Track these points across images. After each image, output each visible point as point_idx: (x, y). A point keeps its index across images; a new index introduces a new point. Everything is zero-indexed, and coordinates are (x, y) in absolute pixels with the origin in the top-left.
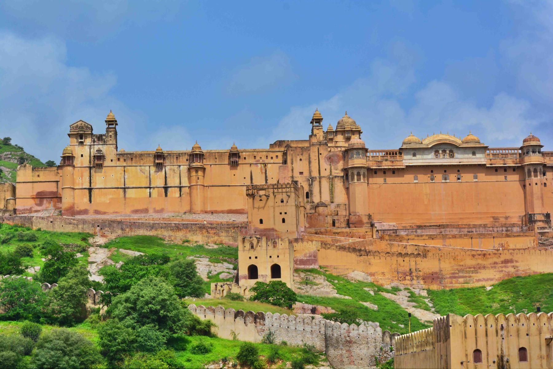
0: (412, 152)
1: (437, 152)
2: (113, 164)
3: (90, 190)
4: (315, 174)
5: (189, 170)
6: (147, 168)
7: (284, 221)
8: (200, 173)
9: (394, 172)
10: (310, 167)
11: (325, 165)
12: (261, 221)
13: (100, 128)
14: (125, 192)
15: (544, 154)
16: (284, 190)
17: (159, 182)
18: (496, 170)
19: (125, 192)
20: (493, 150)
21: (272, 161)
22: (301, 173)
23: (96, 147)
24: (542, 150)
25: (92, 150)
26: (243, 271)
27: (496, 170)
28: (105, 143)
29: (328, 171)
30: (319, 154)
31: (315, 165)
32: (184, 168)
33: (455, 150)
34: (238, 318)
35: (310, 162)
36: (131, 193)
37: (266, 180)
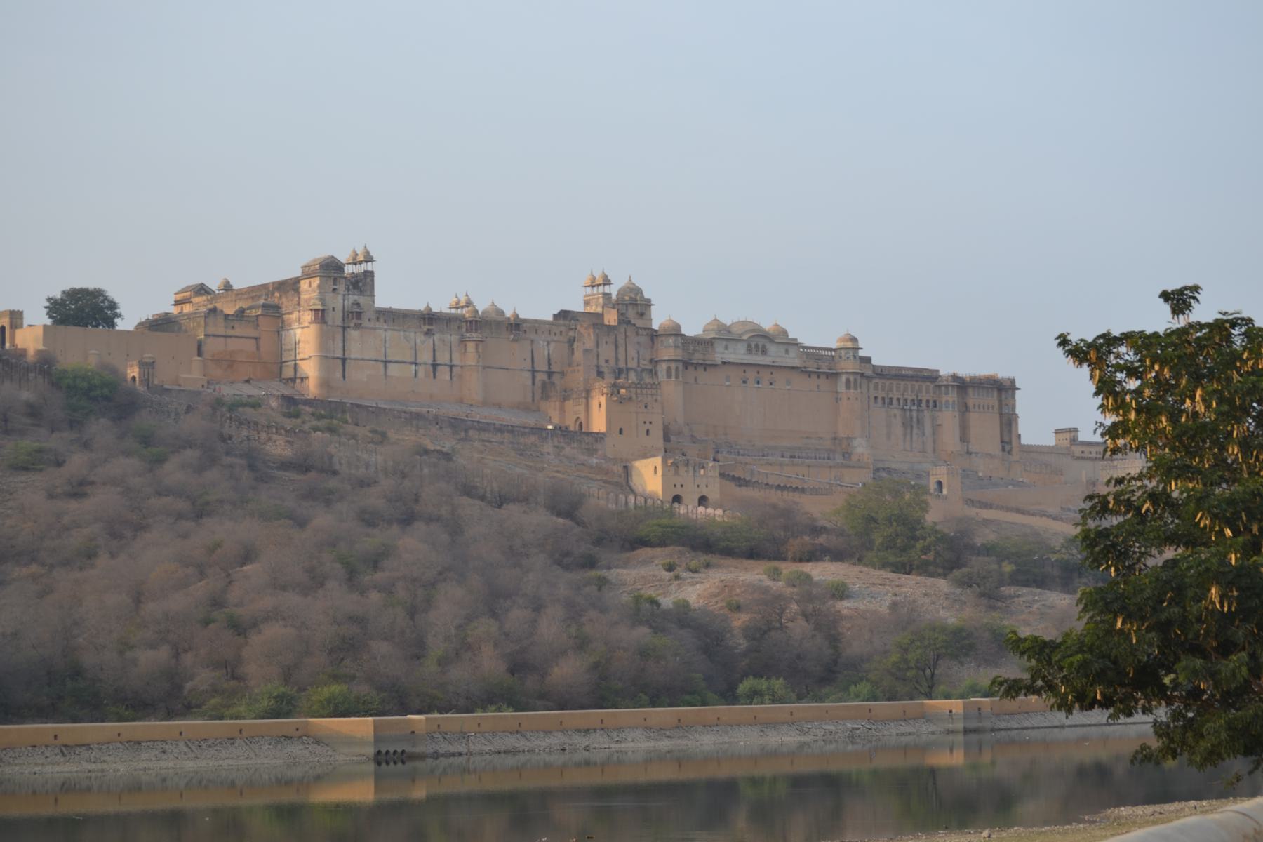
3: (344, 360)
5: (463, 341)
9: (706, 367)
11: (632, 352)
13: (349, 269)
14: (386, 367)
18: (810, 374)
19: (386, 367)
22: (607, 361)
23: (352, 298)
24: (861, 353)
27: (810, 374)
28: (361, 293)
31: (621, 350)
32: (455, 338)
33: (768, 346)
35: (617, 347)
36: (393, 370)
37: (549, 364)
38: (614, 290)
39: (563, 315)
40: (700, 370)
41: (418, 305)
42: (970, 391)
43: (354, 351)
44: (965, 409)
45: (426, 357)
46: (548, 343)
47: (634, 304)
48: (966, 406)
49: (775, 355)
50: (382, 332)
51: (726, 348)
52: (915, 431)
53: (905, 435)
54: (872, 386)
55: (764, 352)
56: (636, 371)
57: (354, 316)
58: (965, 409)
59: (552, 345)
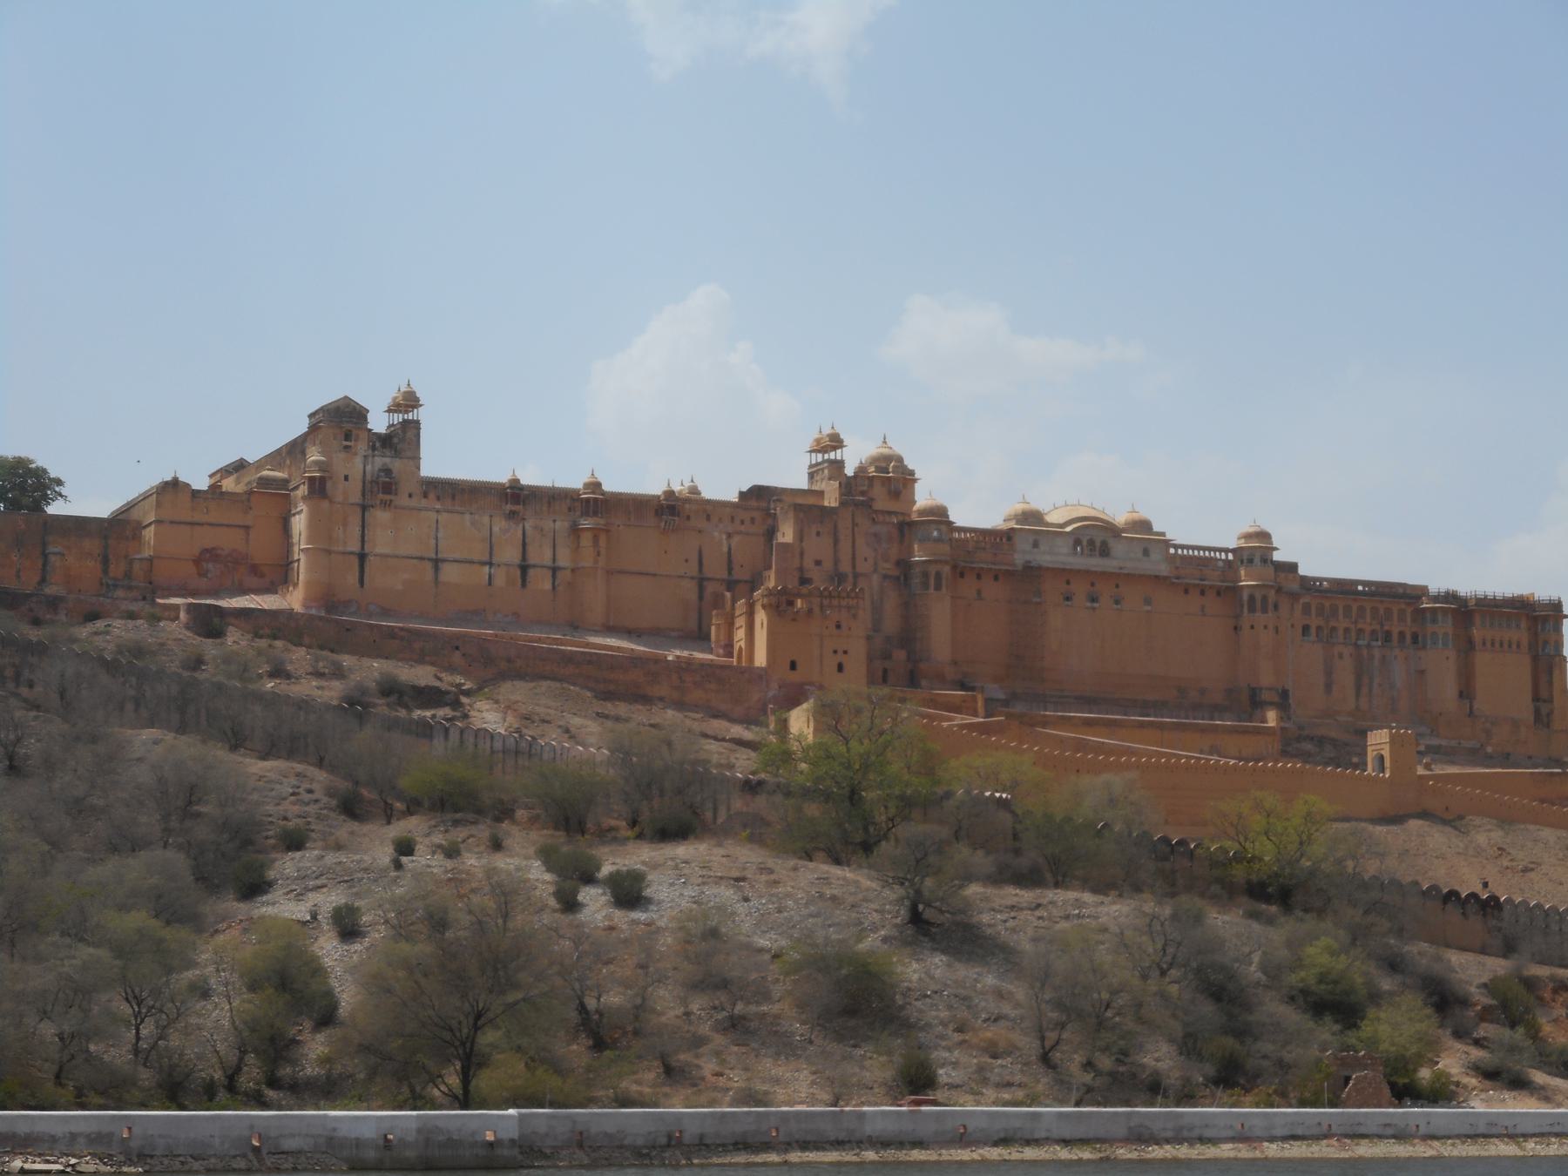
2: (413, 503)
4: (845, 567)
5: (575, 531)
6: (486, 519)
7: (840, 668)
10: (836, 551)
12: (793, 666)
13: (379, 422)
14: (437, 569)
16: (844, 603)
17: (509, 554)
19: (437, 569)
20: (1183, 547)
21: (742, 528)
22: (818, 563)
23: (379, 461)
24: (1277, 556)
25: (369, 468)
28: (397, 453)
30: (855, 525)
31: (845, 546)
32: (562, 525)
33: (1112, 543)
34: (1449, 907)
35: (836, 542)
36: (450, 573)
37: (730, 570)
38: (853, 457)
39: (759, 496)
41: (498, 475)
42: (1477, 619)
43: (381, 542)
44: (1467, 648)
45: (510, 554)
46: (729, 536)
47: (891, 477)
48: (1470, 642)
49: (1122, 558)
50: (433, 515)
54: (1298, 608)
55: (1105, 551)
57: (383, 488)
58: (1467, 648)
59: (736, 540)
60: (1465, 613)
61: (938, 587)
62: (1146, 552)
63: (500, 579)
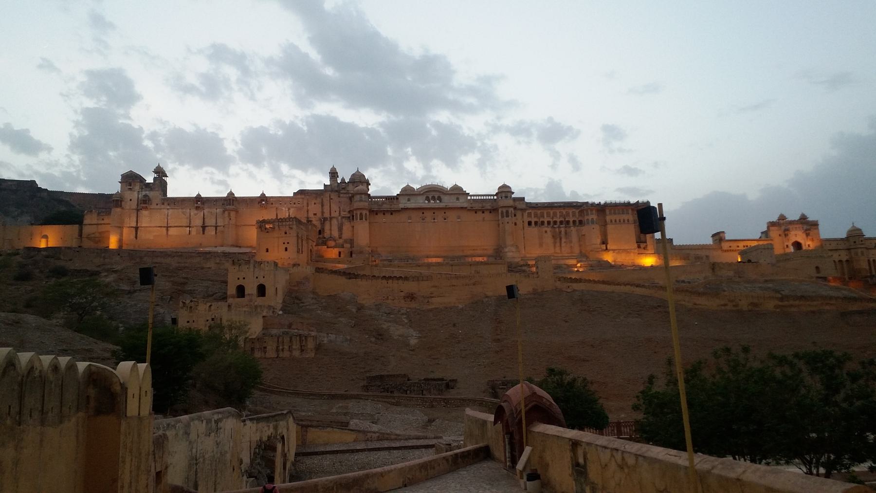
0: (407, 198)
1: (428, 199)
3: (137, 228)
4: (327, 215)
7: (286, 249)
8: (233, 214)
14: (167, 230)
15: (515, 199)
17: (198, 222)
19: (167, 230)
22: (315, 214)
24: (513, 196)
26: (232, 290)
28: (152, 190)
29: (338, 213)
30: (331, 199)
33: (442, 196)
35: (322, 206)
38: (345, 175)
40: (388, 215)
42: (607, 211)
43: (145, 222)
49: (447, 201)
51: (409, 200)
52: (563, 240)
53: (555, 243)
55: (440, 199)
56: (337, 218)
57: (145, 203)
60: (602, 209)
61: (361, 219)
62: (458, 199)
63: (194, 231)
